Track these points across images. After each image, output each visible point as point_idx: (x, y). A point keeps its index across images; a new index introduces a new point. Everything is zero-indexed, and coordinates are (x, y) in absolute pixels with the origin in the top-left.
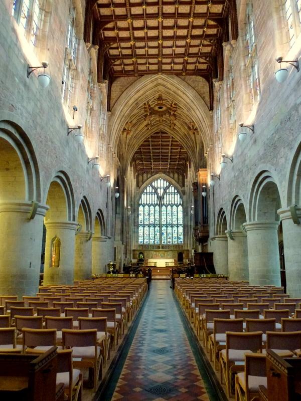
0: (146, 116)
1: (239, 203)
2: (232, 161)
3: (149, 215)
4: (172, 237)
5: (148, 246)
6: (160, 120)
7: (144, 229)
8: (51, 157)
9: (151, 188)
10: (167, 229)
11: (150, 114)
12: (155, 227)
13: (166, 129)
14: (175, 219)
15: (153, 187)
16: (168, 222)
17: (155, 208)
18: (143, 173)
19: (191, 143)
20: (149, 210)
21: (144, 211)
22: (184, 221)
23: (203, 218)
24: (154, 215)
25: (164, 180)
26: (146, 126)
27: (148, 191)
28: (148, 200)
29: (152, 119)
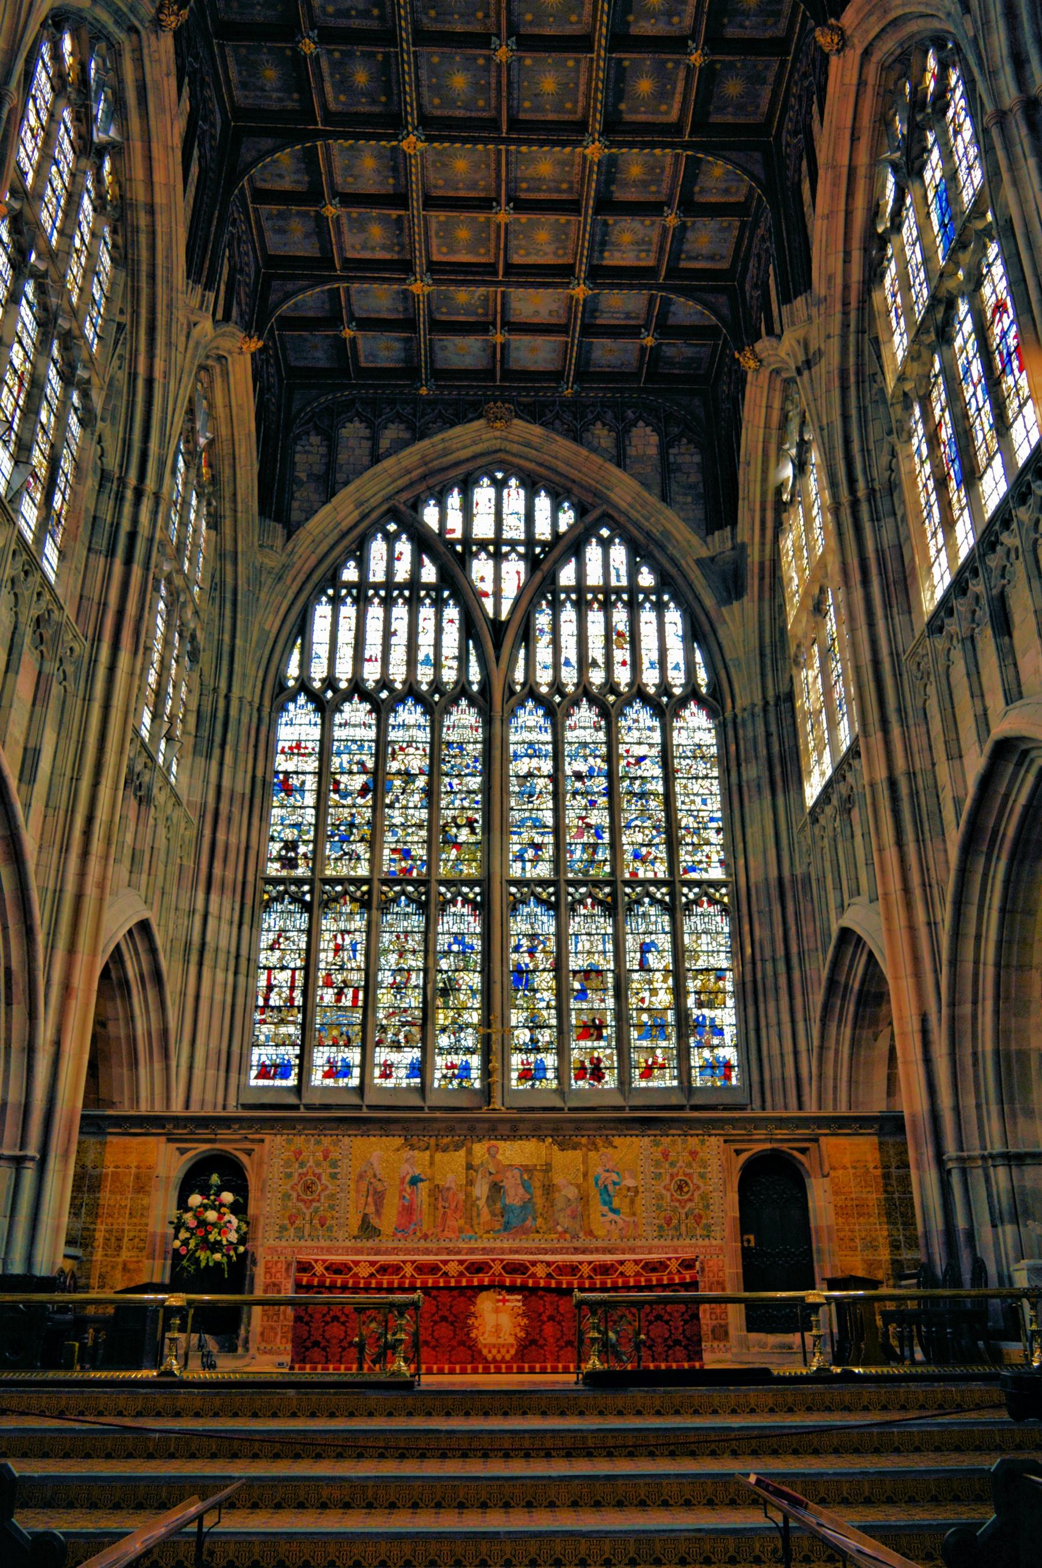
4: (621, 1014)
7: (312, 932)
9: (404, 547)
10: (561, 936)
17: (436, 728)
20: (382, 748)
21: (325, 752)
25: (531, 489)
27: (377, 573)
28: (373, 646)
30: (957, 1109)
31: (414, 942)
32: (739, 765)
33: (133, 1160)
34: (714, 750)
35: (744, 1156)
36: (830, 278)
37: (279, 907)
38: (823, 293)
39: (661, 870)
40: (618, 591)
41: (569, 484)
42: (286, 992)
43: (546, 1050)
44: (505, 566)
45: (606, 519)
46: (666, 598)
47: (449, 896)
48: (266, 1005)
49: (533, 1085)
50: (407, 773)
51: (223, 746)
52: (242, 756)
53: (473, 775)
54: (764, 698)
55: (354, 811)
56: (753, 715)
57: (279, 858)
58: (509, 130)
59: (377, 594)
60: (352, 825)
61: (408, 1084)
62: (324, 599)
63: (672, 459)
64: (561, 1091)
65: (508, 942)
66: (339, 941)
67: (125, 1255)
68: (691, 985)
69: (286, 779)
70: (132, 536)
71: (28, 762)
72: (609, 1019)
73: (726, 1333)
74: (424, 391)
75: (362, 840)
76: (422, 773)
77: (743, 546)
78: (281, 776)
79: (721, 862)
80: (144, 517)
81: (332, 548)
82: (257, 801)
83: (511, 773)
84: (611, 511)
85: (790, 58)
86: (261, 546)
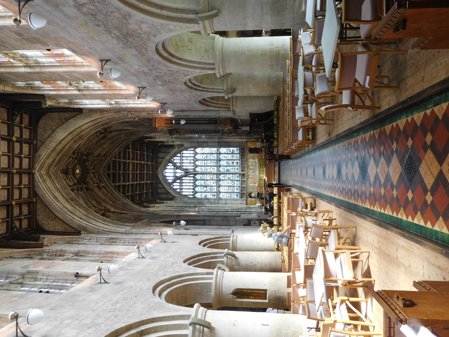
0: (87, 189)
1: (193, 82)
2: (144, 88)
3: (206, 186)
5: (242, 187)
6: (93, 173)
8: (135, 303)
9: (174, 184)
11: (85, 183)
13: (104, 165)
14: (212, 157)
15: (174, 181)
16: (214, 164)
17: (199, 180)
18: (157, 193)
19: (123, 135)
22: (214, 147)
23: (211, 124)
24: (207, 180)
25: (166, 169)
26: (100, 189)
27: (179, 187)
28: (188, 187)
29: (91, 182)
31: (224, 181)
39: (216, 155)
40: (181, 158)
44: (177, 172)
45: (171, 160)
64: (239, 166)
68: (228, 152)
72: (232, 161)
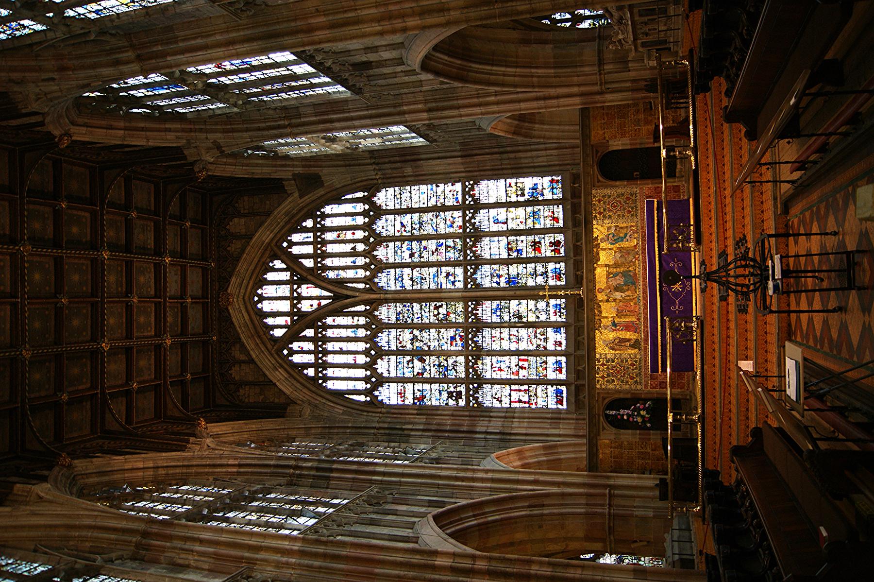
3: (420, 354)
7: (493, 382)
9: (295, 346)
10: (491, 262)
12: (480, 325)
15: (294, 334)
16: (452, 255)
17: (389, 326)
20: (400, 352)
24: (423, 327)
27: (310, 358)
28: (349, 359)
30: (579, 85)
31: (496, 332)
32: (405, 177)
33: (607, 451)
34: (397, 189)
35: (601, 179)
36: (178, 138)
37: (481, 399)
38: (185, 141)
40: (315, 237)
41: (261, 263)
42: (522, 393)
43: (546, 268)
44: (304, 294)
46: (319, 213)
47: (473, 317)
48: (528, 402)
49: (563, 274)
50: (412, 340)
51: (401, 429)
52: (408, 420)
53: (412, 308)
54: (371, 164)
55: (432, 365)
56: (379, 170)
57: (457, 400)
58: (97, 297)
59: (321, 358)
60: (439, 366)
61: (565, 333)
62: (324, 384)
63: (246, 211)
65: (495, 288)
66: (497, 369)
67: (649, 450)
68: (514, 199)
69: (418, 399)
70: (318, 469)
71: (436, 505)
72: (531, 238)
73: (676, 186)
74: (215, 338)
75: (446, 360)
76: (412, 332)
77: (294, 175)
78: (416, 401)
79: (452, 185)
80: (309, 464)
81: (298, 381)
82: (429, 412)
83: (411, 288)
84: (274, 242)
85: (63, 158)
86: (300, 417)
